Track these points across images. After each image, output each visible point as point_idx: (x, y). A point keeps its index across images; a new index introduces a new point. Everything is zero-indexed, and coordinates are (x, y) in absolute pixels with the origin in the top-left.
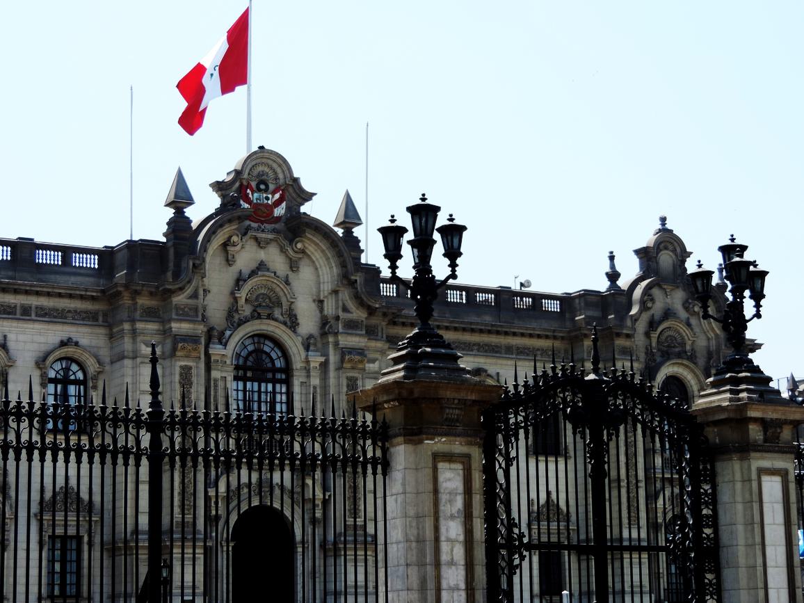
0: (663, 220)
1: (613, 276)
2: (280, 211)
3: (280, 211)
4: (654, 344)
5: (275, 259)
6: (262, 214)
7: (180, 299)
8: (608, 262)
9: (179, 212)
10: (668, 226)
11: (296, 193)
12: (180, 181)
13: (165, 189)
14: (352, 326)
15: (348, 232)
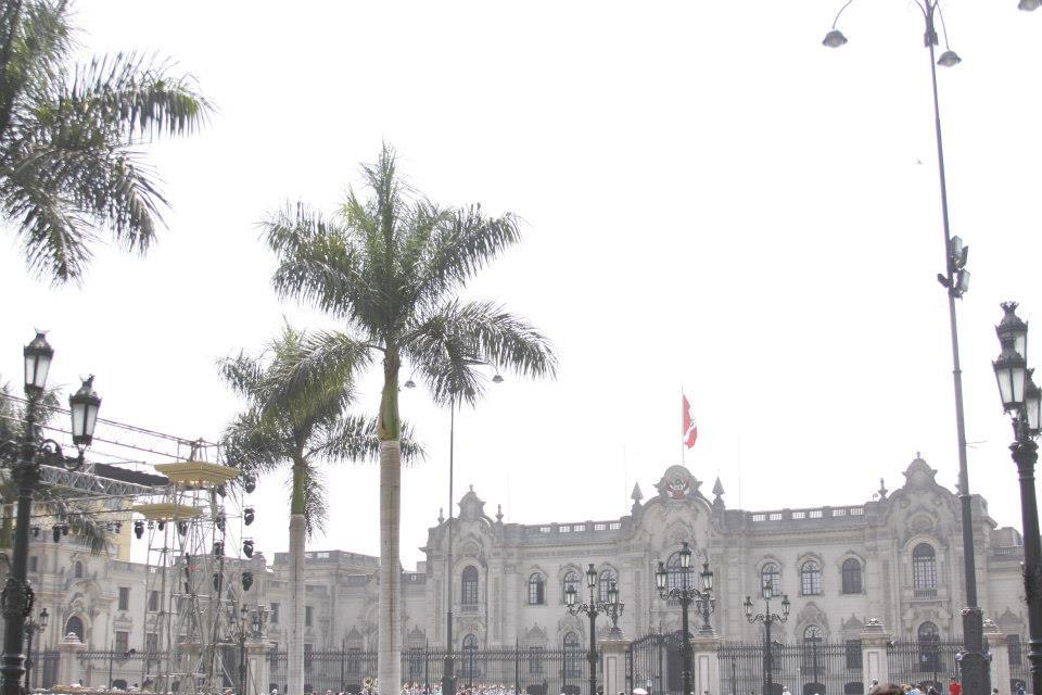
0: (919, 454)
1: (883, 492)
2: (686, 492)
3: (686, 492)
4: (910, 526)
5: (686, 515)
6: (678, 495)
7: (632, 542)
8: (880, 484)
9: (637, 502)
10: (921, 457)
11: (694, 484)
12: (637, 487)
13: (630, 493)
14: (716, 543)
15: (718, 497)
